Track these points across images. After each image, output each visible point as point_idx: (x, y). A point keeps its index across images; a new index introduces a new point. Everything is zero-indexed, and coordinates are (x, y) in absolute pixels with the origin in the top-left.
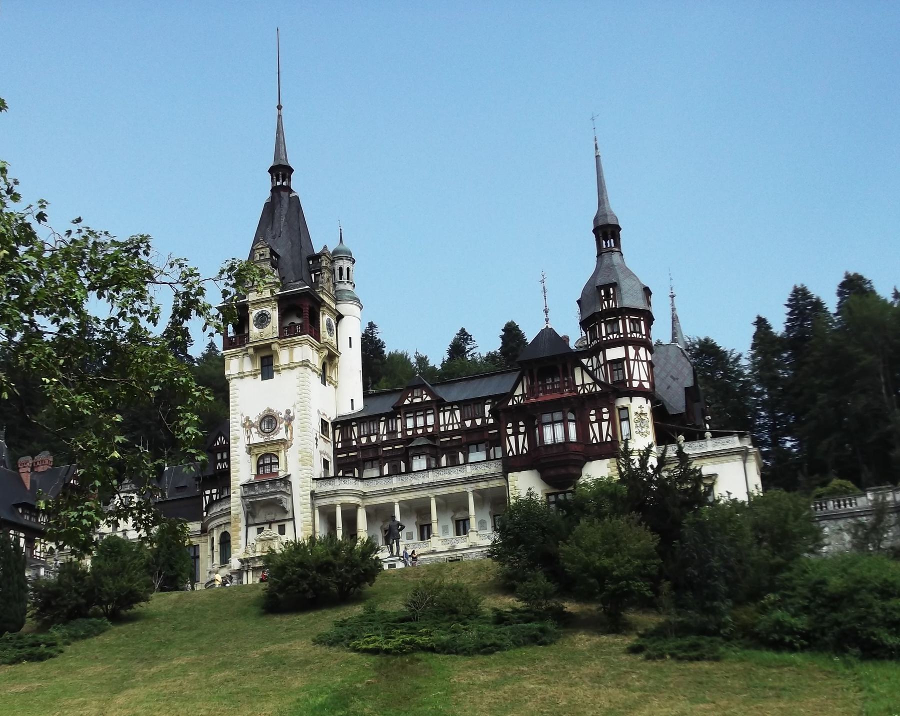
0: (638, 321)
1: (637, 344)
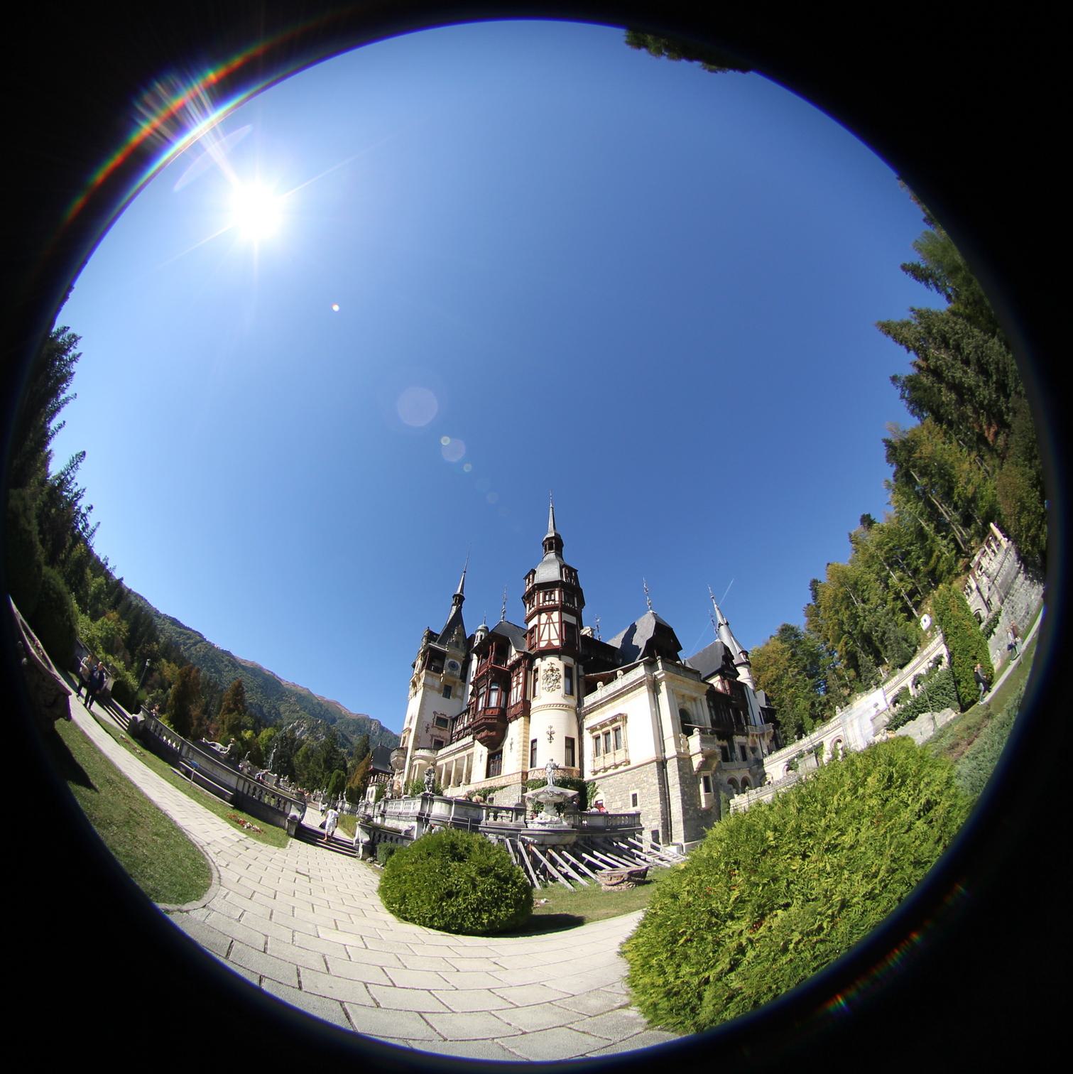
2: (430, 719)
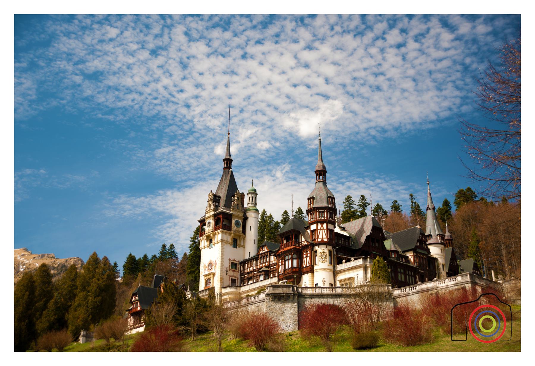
0: (324, 212)
1: (322, 222)
2: (227, 264)
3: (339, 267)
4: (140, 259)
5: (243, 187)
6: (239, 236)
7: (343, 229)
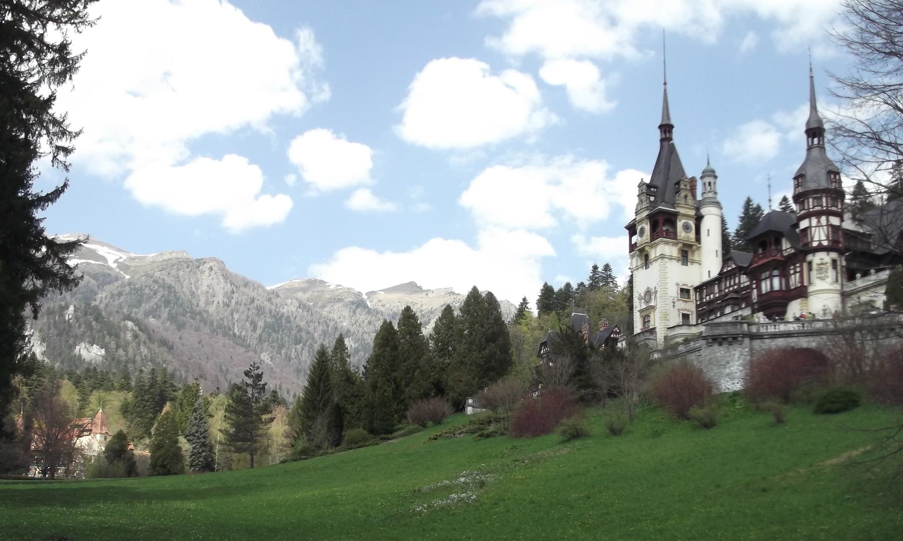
0: (820, 198)
1: (818, 214)
2: (674, 292)
3: (849, 287)
4: (561, 290)
5: (692, 168)
6: (690, 246)
7: (860, 222)
